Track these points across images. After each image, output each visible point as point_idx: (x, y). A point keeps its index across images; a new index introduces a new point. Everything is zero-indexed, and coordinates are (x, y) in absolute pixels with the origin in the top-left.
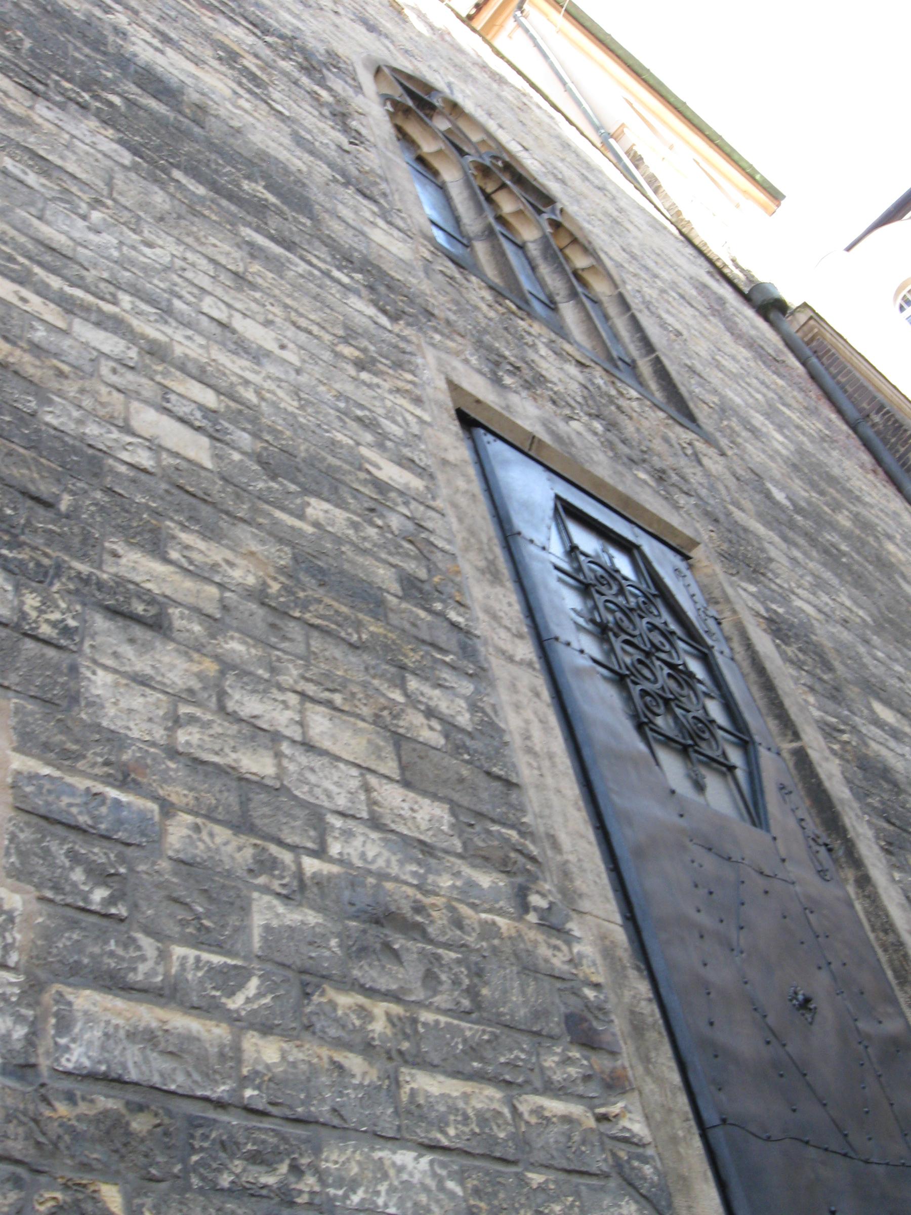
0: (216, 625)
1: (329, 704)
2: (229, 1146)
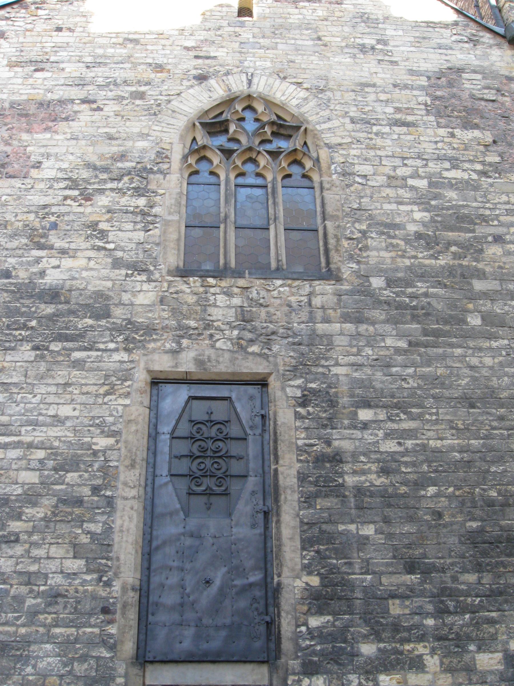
0: (30, 534)
1: (58, 543)
2: (13, 648)
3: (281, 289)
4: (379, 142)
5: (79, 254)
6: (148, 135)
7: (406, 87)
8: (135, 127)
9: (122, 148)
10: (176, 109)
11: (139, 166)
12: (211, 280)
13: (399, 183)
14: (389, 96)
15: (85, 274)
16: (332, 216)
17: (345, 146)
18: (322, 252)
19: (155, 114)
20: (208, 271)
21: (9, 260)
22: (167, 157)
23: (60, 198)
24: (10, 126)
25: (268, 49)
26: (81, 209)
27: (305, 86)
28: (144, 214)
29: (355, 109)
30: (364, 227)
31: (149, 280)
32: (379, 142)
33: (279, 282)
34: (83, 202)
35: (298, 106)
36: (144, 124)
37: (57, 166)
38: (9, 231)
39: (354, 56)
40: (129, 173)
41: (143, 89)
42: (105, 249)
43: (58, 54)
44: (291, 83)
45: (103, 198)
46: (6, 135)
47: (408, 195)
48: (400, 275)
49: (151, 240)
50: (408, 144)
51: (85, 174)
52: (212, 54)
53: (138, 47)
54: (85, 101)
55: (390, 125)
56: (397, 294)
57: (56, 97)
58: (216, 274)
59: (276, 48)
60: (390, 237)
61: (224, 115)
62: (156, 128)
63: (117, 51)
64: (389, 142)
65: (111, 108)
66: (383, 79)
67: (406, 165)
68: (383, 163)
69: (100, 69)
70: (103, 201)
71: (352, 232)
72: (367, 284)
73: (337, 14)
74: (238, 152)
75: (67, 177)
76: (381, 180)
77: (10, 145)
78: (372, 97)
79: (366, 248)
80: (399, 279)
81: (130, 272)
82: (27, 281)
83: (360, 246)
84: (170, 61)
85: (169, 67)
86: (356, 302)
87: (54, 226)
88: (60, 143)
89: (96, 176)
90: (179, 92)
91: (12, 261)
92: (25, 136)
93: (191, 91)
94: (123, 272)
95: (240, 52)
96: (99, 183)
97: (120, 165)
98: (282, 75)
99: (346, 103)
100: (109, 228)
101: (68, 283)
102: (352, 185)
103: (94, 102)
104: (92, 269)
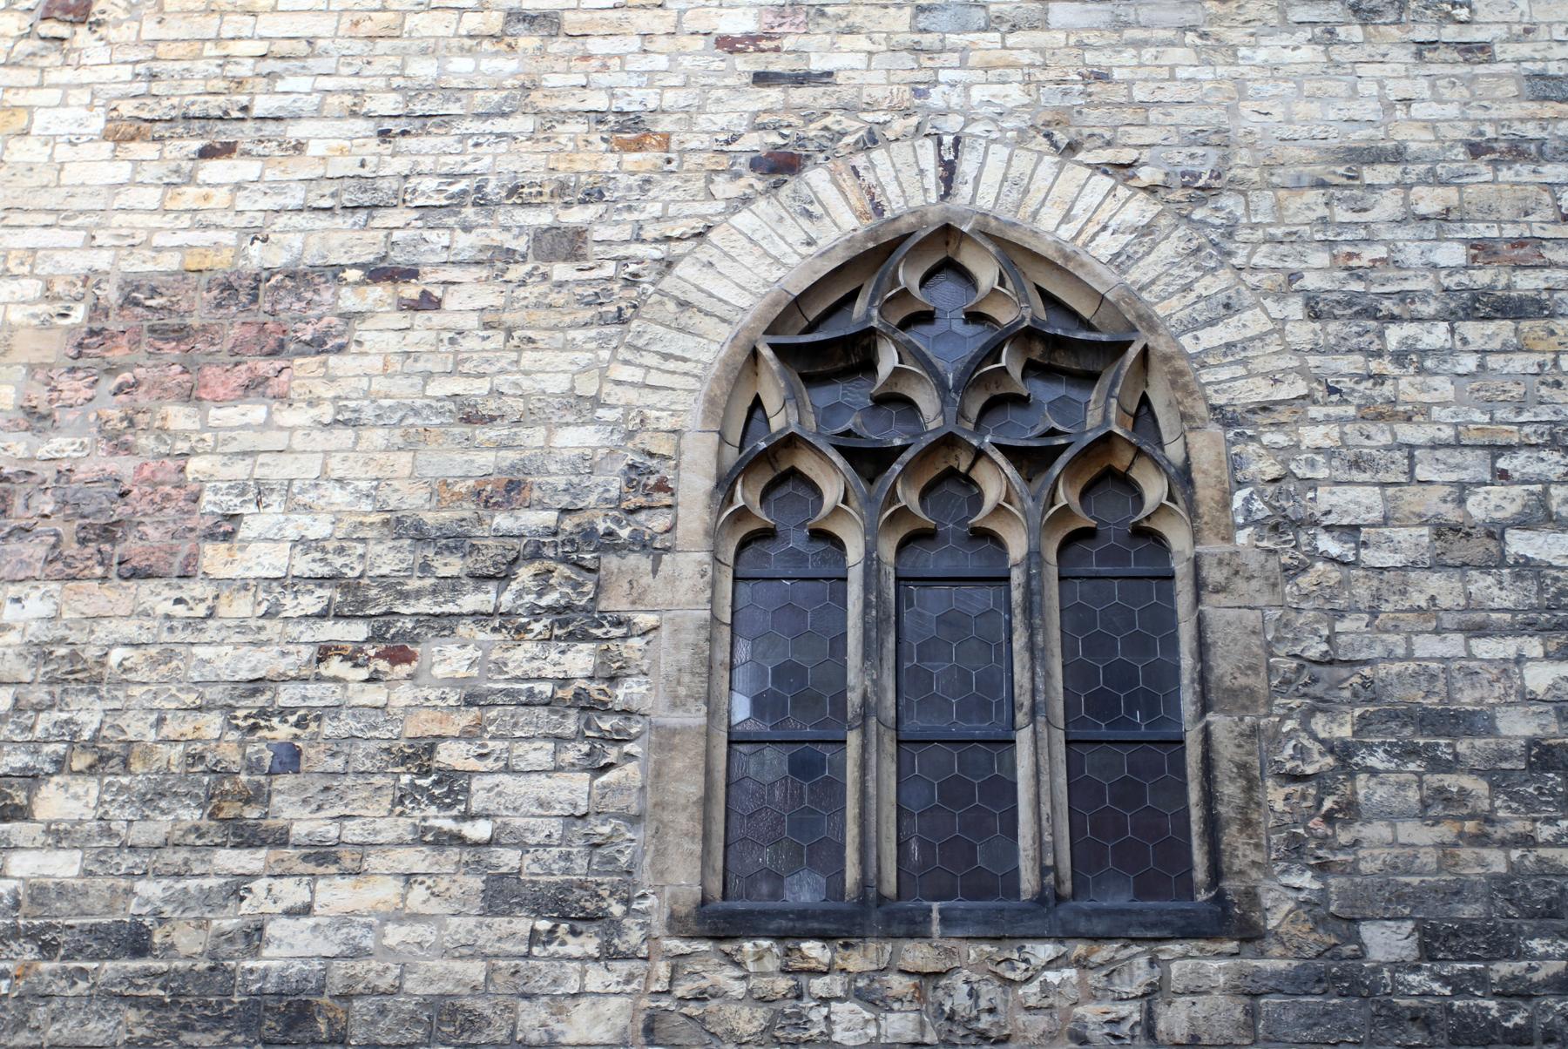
3: (1052, 977)
4: (1408, 388)
5: (374, 862)
6: (597, 402)
7: (1517, 151)
8: (553, 371)
9: (511, 456)
10: (694, 296)
11: (569, 524)
12: (813, 949)
13: (1477, 549)
14: (1451, 195)
15: (395, 935)
16: (1233, 693)
17: (1283, 415)
18: (1196, 827)
19: (620, 319)
20: (803, 914)
21: (140, 886)
22: (662, 486)
23: (307, 653)
24: (127, 376)
25: (1014, 28)
26: (375, 695)
27: (1146, 175)
28: (588, 706)
29: (1321, 258)
30: (1345, 732)
31: (609, 955)
32: (1408, 388)
33: (1043, 951)
34: (383, 665)
35: (1119, 261)
36: (583, 358)
37: (291, 533)
38: (138, 778)
39: (1328, 36)
40: (537, 555)
41: (576, 216)
42: (459, 840)
43: (280, 86)
44: (1096, 167)
45: (451, 649)
46: (114, 413)
47: (1508, 598)
48: (1469, 911)
49: (615, 803)
50: (1517, 391)
51: (388, 559)
52: (817, 65)
53: (558, 46)
54: (379, 273)
55: (1450, 317)
56: (1458, 985)
57: (278, 258)
58: (830, 927)
60: (1437, 765)
61: (860, 306)
62: (624, 373)
63: (487, 65)
64: (1443, 388)
65: (470, 296)
66: (1431, 125)
67: (1503, 476)
68: (1421, 473)
69: (427, 143)
70: (449, 660)
71: (1301, 753)
72: (1348, 949)
74: (907, 456)
75: (324, 571)
76: (1412, 539)
77: (128, 448)
78: (1388, 205)
79: (1350, 811)
80: (1468, 927)
81: (544, 925)
82: (202, 965)
83: (1328, 804)
84: (670, 98)
85: (665, 125)
86: (1312, 1019)
87: (289, 759)
88: (298, 441)
89: (426, 567)
90: (700, 226)
91: (150, 889)
92: (179, 417)
93: (743, 219)
94: (522, 925)
95: (916, 49)
96: (434, 592)
97: (502, 521)
98: (1061, 138)
99: (1293, 238)
100: (473, 764)
101: (340, 969)
102: (1304, 569)
103: (411, 274)
104: (416, 917)
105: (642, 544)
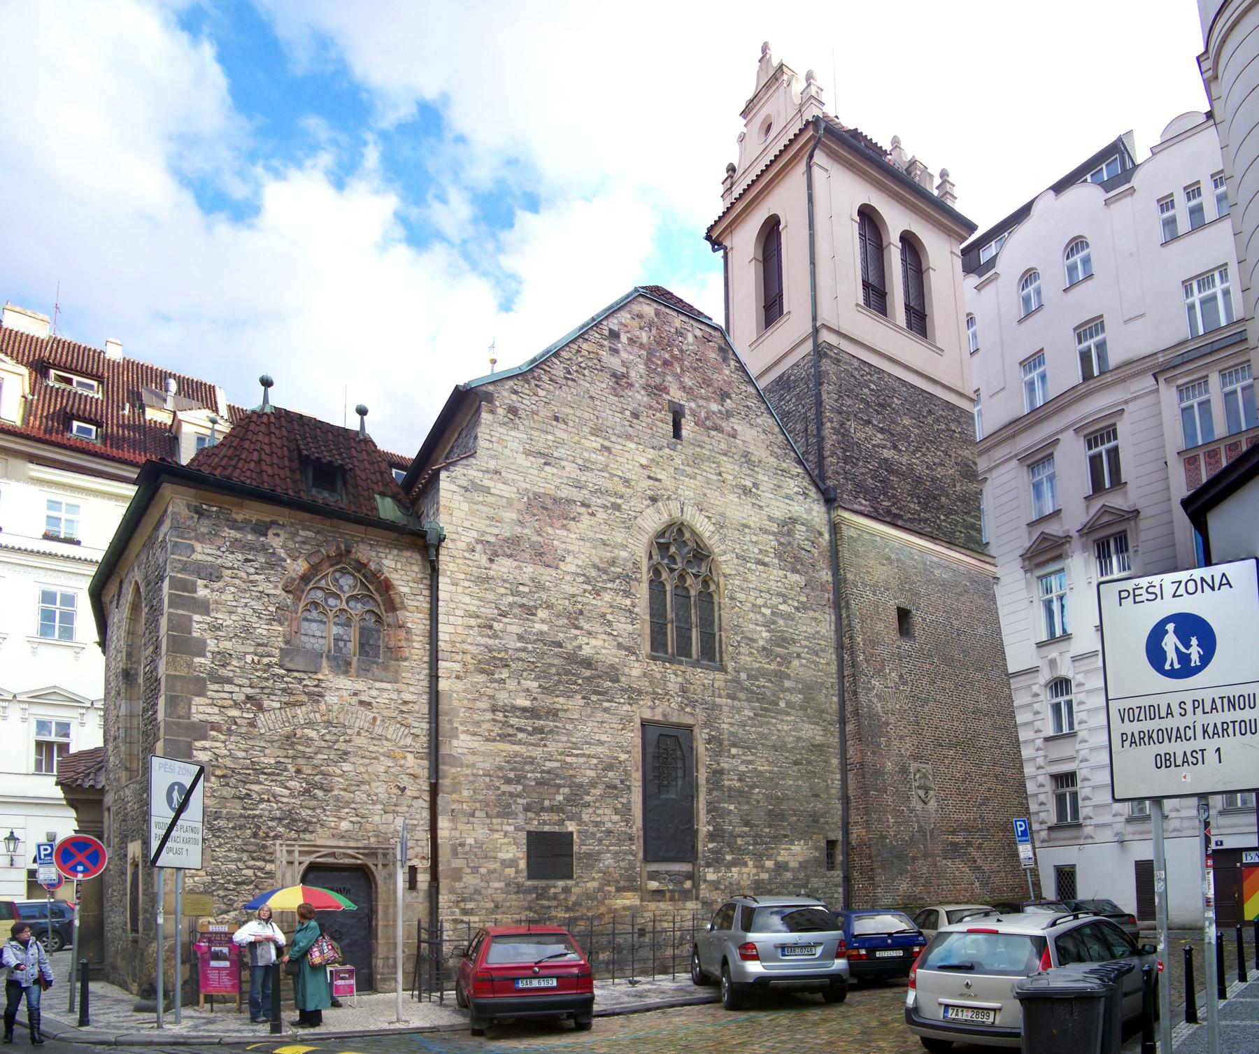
8: (619, 536)
26: (594, 602)
27: (713, 521)
35: (709, 538)
41: (619, 501)
51: (594, 573)
52: (659, 477)
59: (695, 479)
70: (607, 597)
73: (734, 450)
78: (747, 538)
87: (581, 613)
103: (588, 506)
105: (636, 579)
